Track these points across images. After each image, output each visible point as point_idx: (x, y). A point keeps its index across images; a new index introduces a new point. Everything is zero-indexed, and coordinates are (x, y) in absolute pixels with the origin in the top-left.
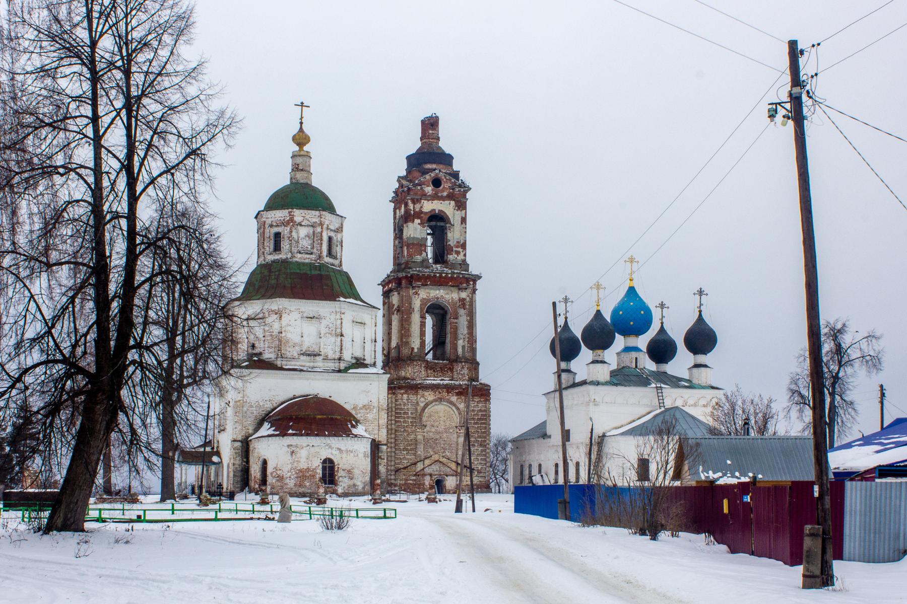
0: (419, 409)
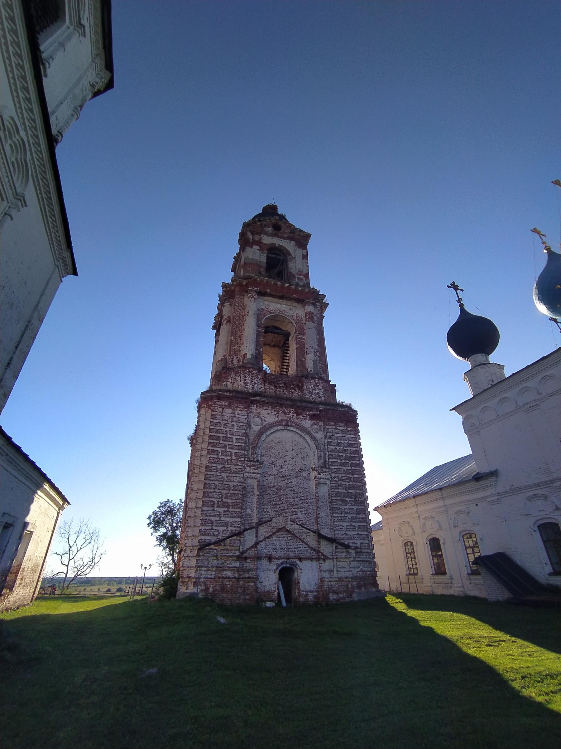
0: (252, 434)
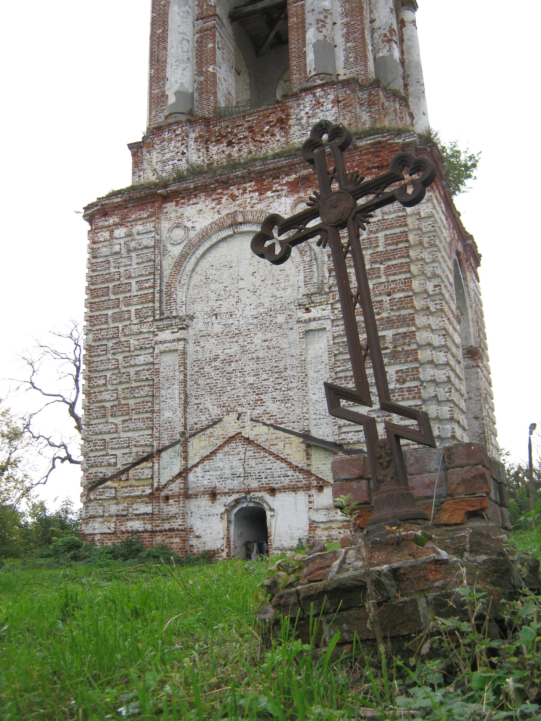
0: (168, 264)
